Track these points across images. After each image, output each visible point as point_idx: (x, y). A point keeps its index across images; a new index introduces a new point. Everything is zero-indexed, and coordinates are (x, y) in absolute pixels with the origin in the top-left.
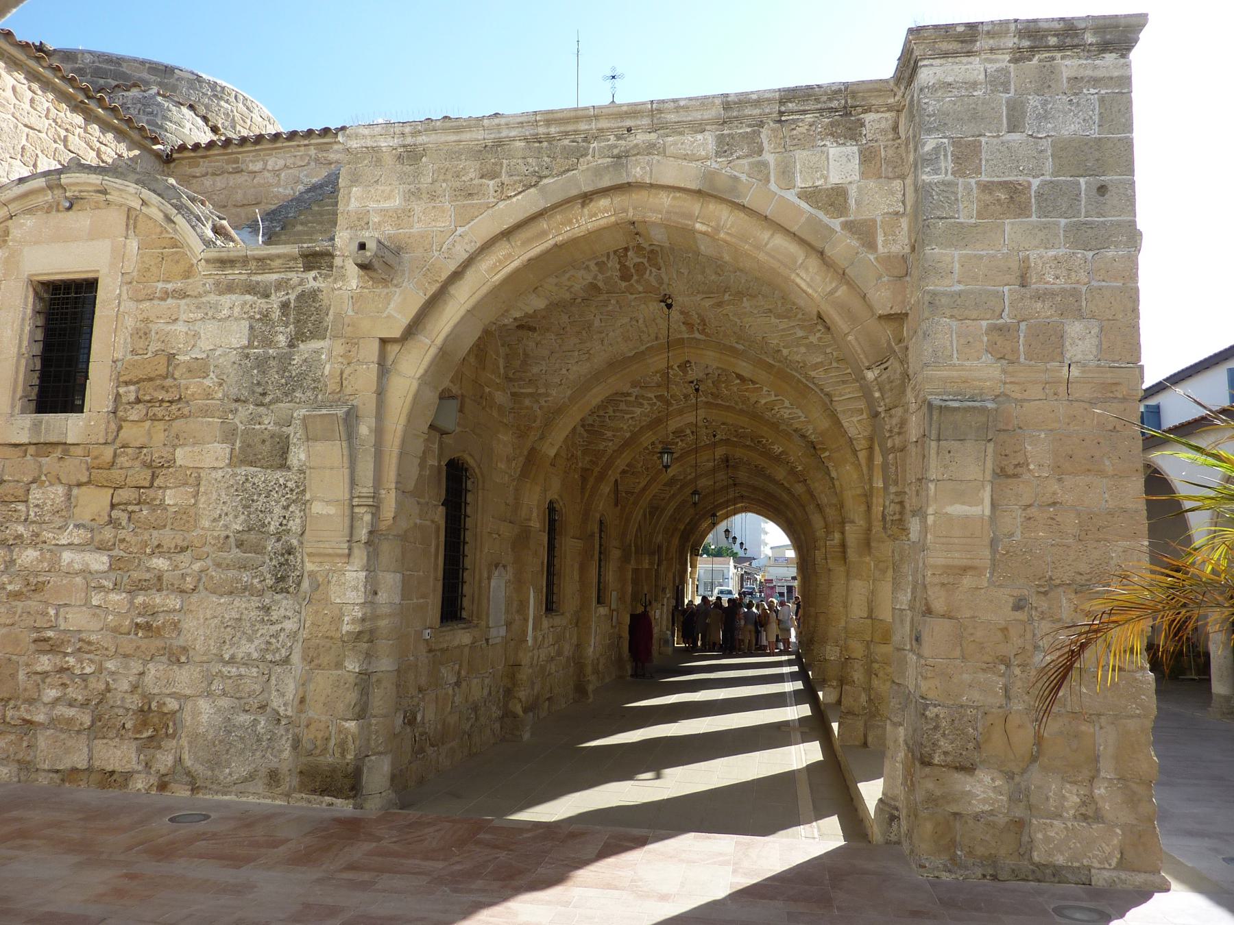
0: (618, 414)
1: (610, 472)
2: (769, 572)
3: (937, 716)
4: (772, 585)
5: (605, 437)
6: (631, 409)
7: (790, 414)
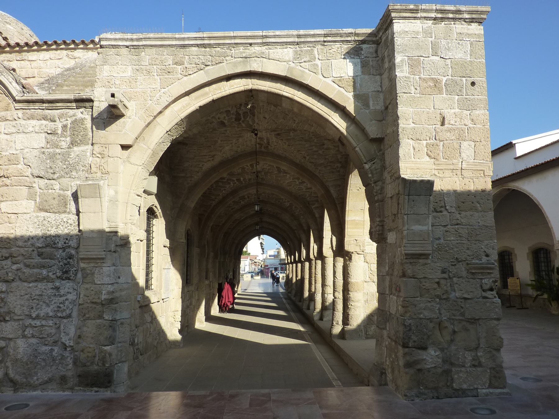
1: (213, 216)
3: (410, 324)
4: (268, 267)
7: (298, 188)
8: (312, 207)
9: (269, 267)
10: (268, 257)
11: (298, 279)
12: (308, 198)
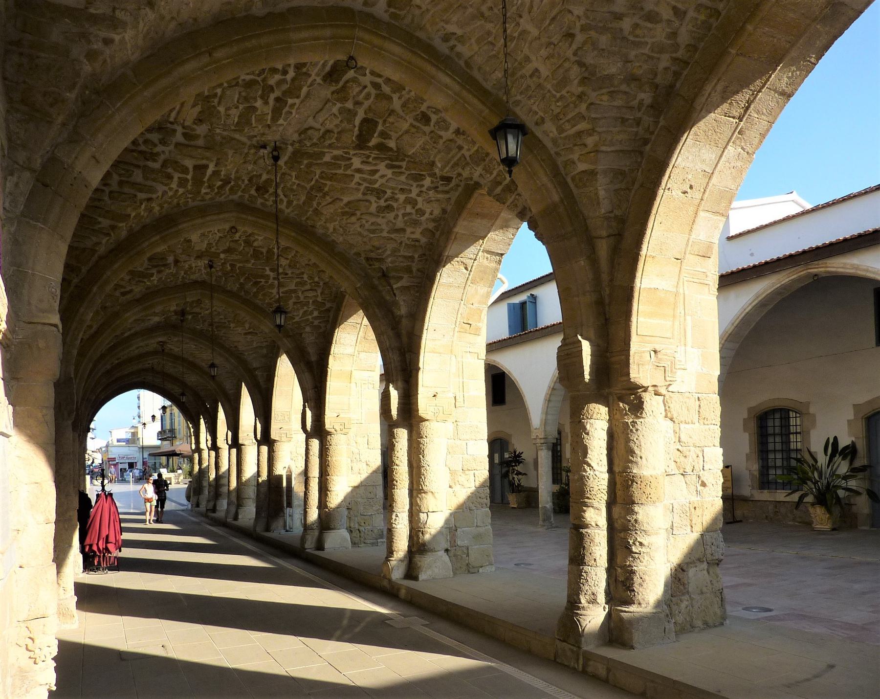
0: (126, 190)
1: (95, 289)
2: (111, 452)
4: (115, 462)
5: (97, 227)
6: (149, 183)
7: (372, 224)
8: (395, 286)
9: (117, 461)
10: (115, 443)
11: (260, 480)
12: (390, 259)
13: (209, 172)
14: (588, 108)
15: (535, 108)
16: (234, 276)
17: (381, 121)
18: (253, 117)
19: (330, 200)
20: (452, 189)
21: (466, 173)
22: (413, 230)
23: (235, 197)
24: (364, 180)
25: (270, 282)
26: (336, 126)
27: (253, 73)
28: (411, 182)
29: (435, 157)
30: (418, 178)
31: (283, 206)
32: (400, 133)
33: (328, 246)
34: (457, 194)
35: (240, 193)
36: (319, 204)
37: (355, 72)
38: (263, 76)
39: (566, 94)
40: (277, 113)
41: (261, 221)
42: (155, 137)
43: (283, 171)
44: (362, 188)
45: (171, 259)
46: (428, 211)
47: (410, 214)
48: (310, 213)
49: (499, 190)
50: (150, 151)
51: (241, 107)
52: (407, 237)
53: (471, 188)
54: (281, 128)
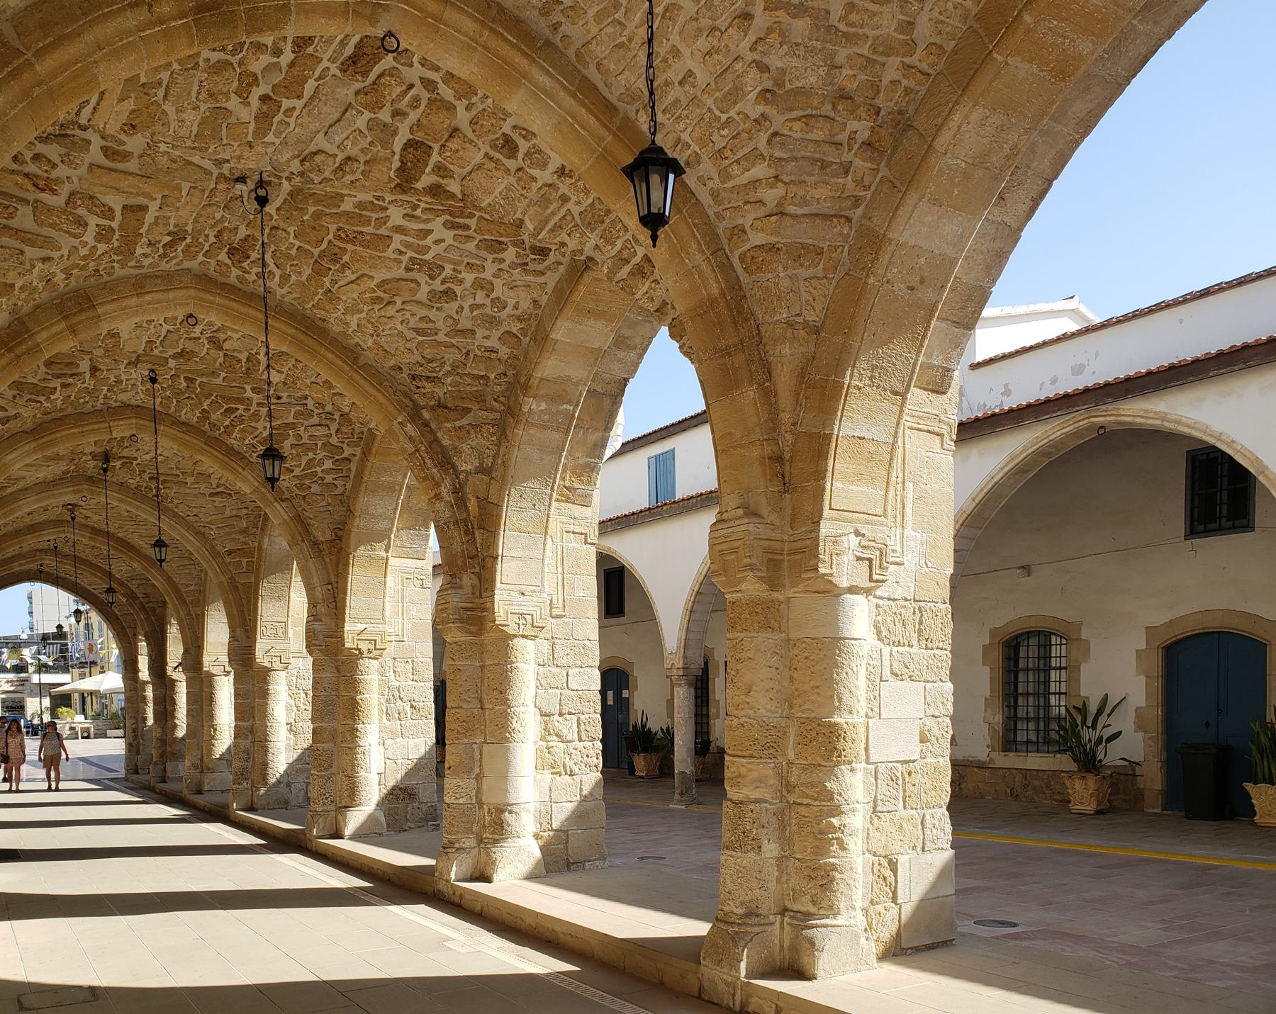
13: (149, 218)
14: (769, 142)
15: (685, 137)
16: (192, 398)
17: (436, 147)
18: (224, 125)
19: (353, 277)
20: (548, 268)
21: (572, 244)
22: (488, 333)
23: (193, 264)
24: (408, 245)
25: (254, 408)
26: (363, 150)
27: (223, 49)
28: (484, 254)
29: (524, 213)
30: (496, 247)
31: (273, 284)
32: (468, 169)
33: (349, 354)
34: (557, 276)
35: (200, 258)
36: (333, 282)
37: (395, 59)
38: (241, 55)
39: (736, 117)
40: (264, 119)
41: (235, 305)
42: (53, 151)
43: (273, 223)
44: (405, 259)
45: (85, 366)
46: (511, 302)
47: (482, 306)
48: (319, 296)
49: (624, 272)
50: (46, 175)
51: (203, 107)
52: (476, 344)
53: (581, 267)
54: (270, 150)
